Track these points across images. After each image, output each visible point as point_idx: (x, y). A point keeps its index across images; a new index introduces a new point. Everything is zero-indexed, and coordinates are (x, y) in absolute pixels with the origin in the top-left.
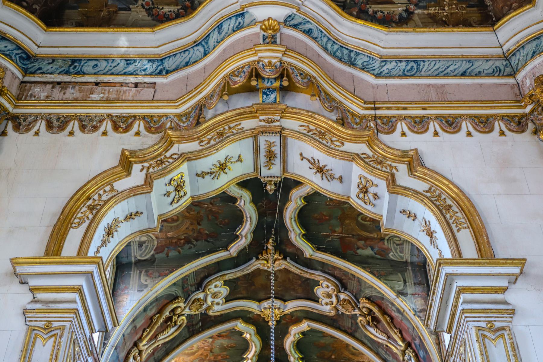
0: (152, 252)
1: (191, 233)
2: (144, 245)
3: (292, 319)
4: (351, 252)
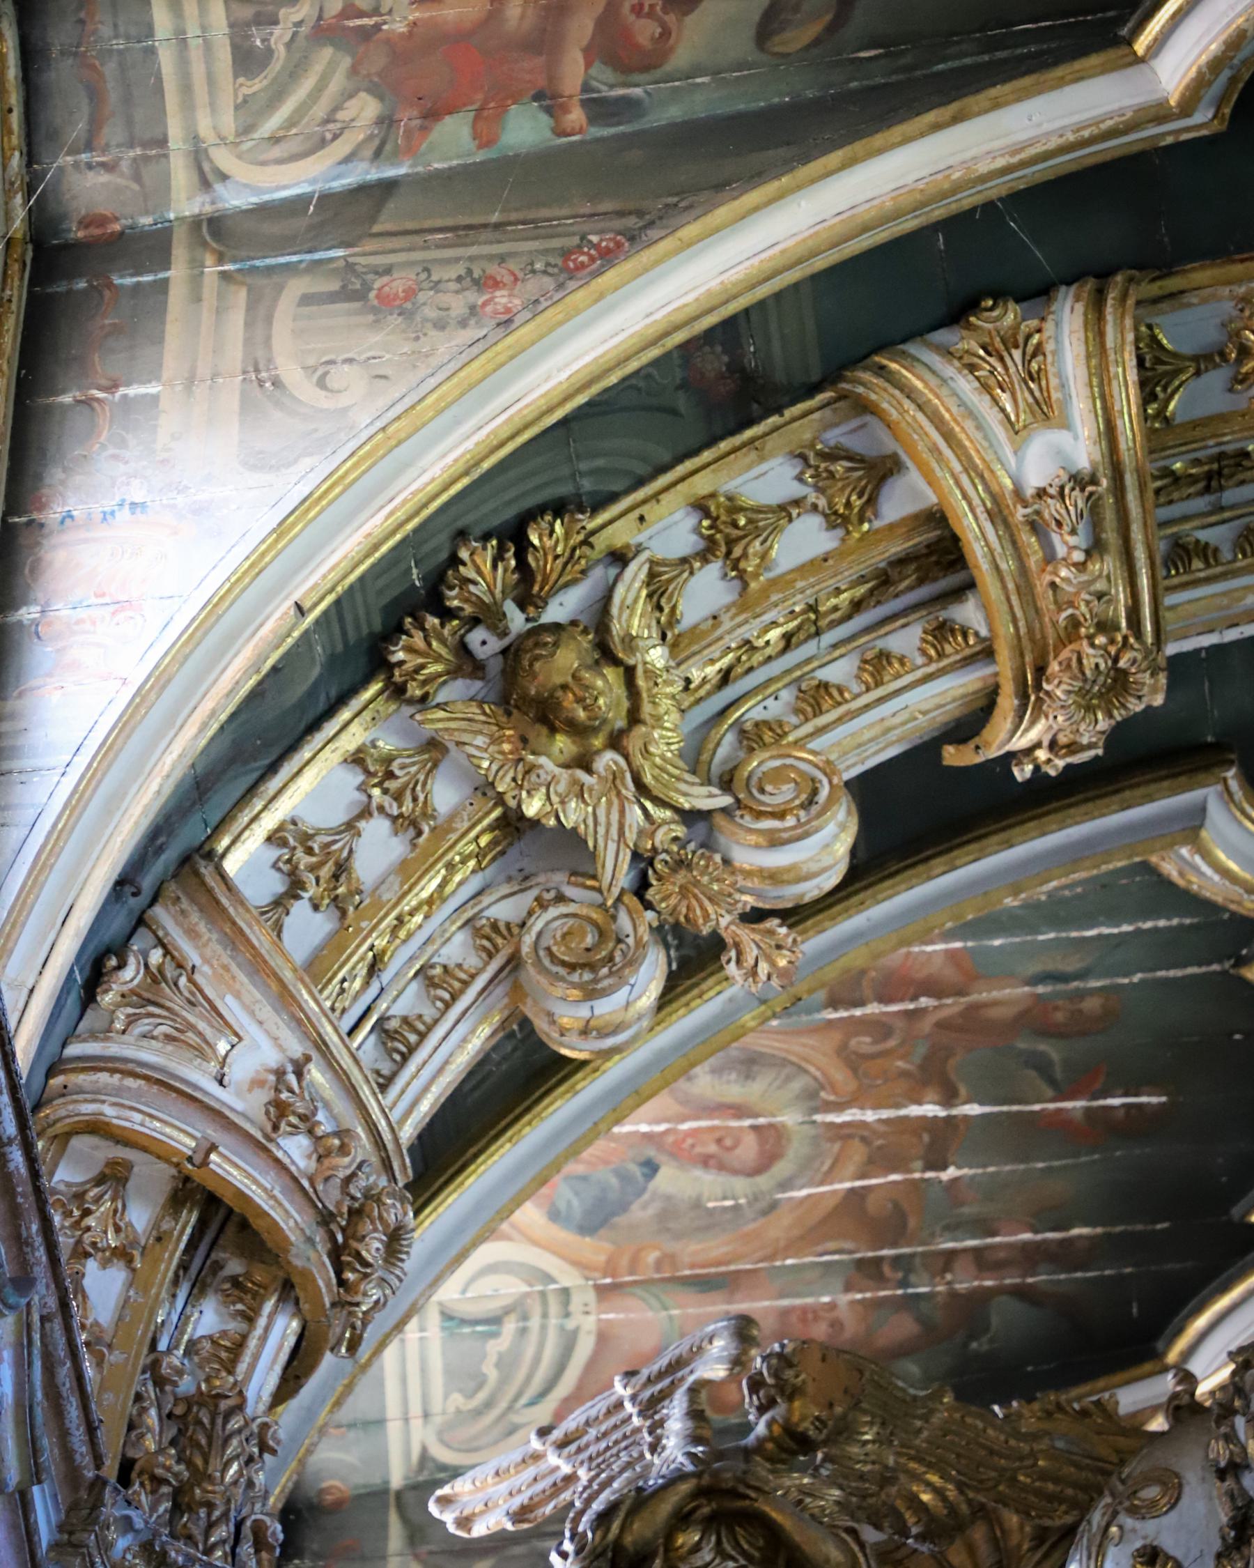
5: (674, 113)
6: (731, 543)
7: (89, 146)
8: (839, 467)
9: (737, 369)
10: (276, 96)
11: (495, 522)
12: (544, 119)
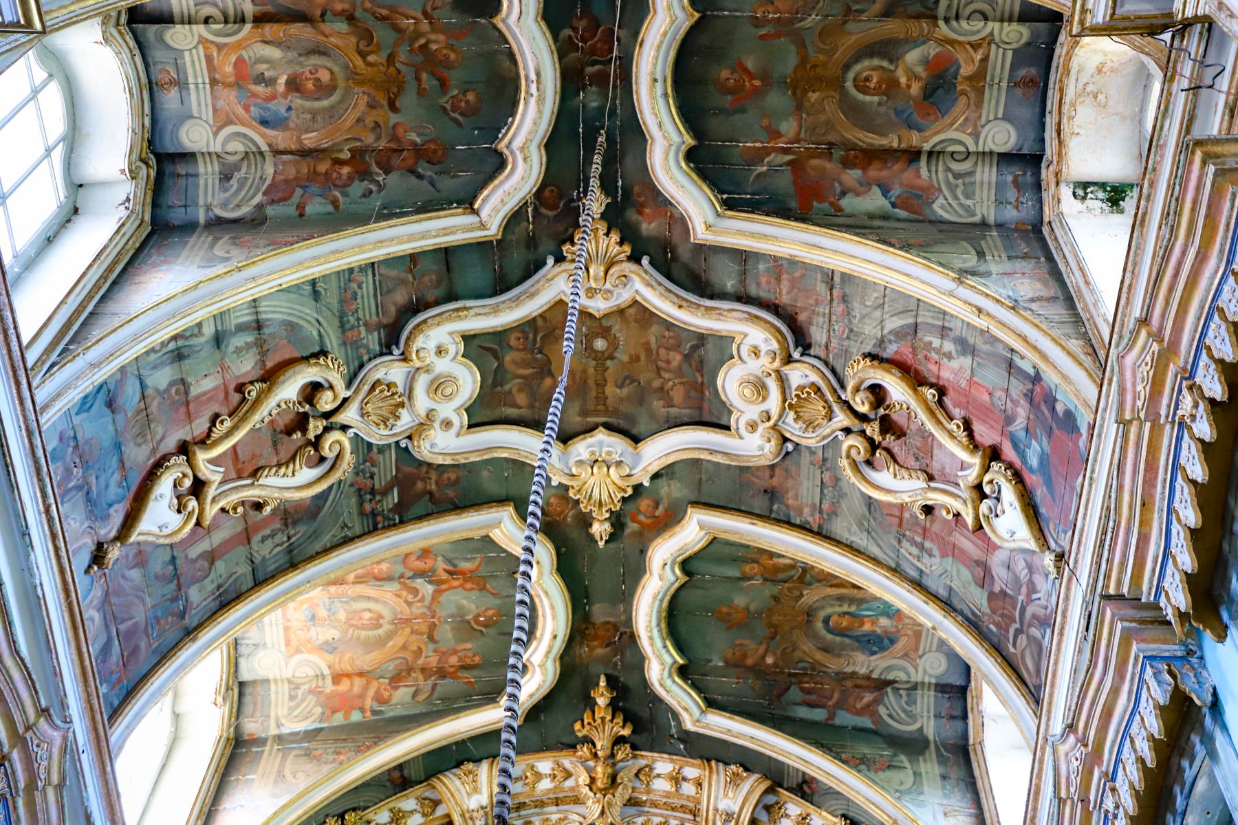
0: (258, 198)
1: (369, 139)
2: (237, 175)
3: (657, 513)
4: (825, 206)
5: (391, 714)
6: (397, 820)
7: (252, 717)
8: (426, 802)
9: (402, 776)
10: (298, 706)
11: (337, 812)
12: (361, 715)
